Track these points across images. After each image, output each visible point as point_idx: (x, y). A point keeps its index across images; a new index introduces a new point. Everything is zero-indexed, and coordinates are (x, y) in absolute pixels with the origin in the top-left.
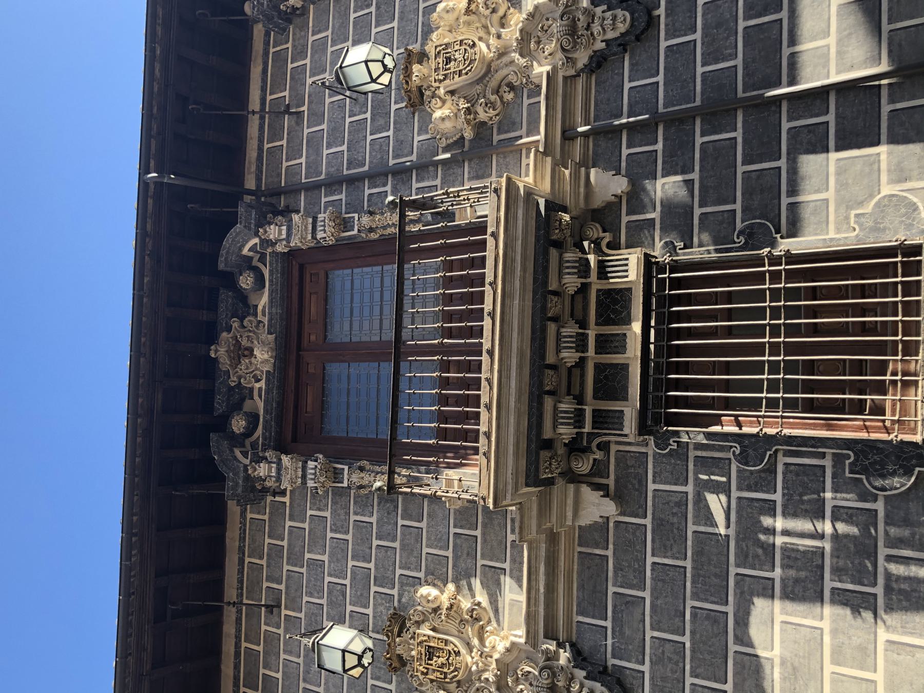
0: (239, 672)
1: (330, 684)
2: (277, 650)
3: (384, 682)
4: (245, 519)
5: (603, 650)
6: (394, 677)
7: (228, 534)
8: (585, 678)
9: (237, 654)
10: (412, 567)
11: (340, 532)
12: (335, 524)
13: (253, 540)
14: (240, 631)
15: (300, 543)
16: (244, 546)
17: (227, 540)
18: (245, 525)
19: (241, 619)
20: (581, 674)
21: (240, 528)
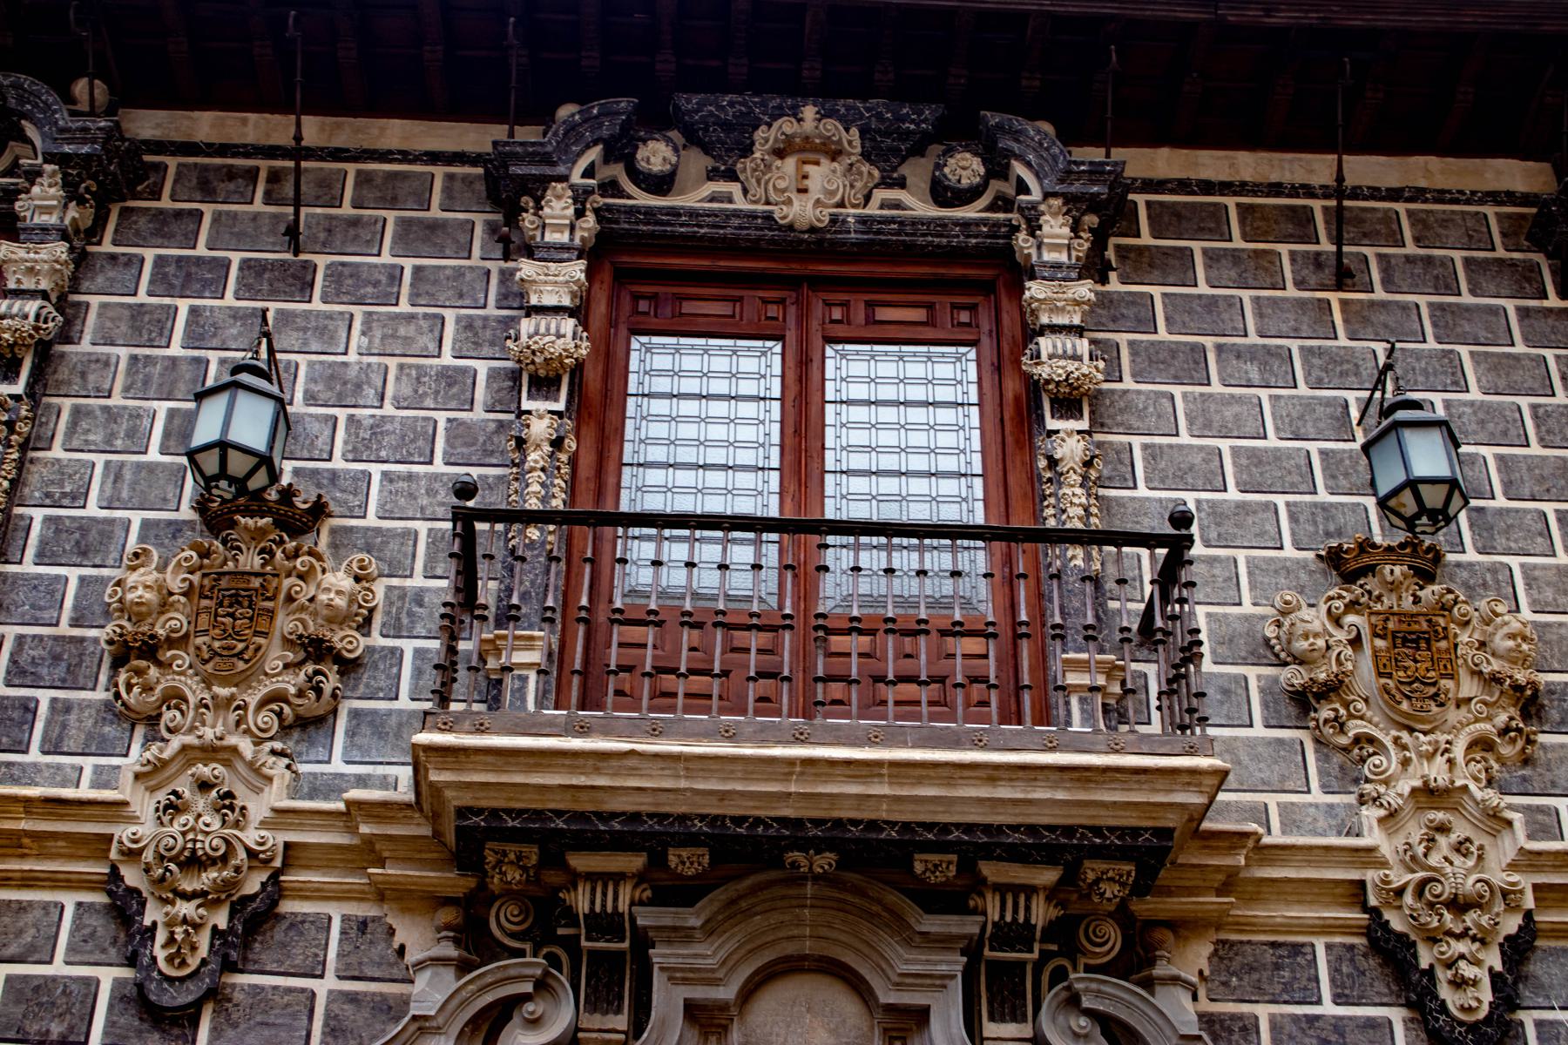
0: (1172, 192)
1: (1236, 409)
2: (1251, 282)
3: (1293, 534)
4: (1481, 202)
5: (1541, 1001)
6: (1310, 555)
7: (1433, 161)
8: (1491, 969)
9: (1207, 187)
10: (1534, 592)
11: (1538, 426)
12: (1548, 415)
13: (1446, 221)
14: (1255, 194)
15: (1483, 335)
16: (1426, 201)
17: (1421, 159)
18: (1468, 202)
19: (1278, 195)
20: (1494, 959)
21: (1461, 192)
